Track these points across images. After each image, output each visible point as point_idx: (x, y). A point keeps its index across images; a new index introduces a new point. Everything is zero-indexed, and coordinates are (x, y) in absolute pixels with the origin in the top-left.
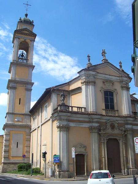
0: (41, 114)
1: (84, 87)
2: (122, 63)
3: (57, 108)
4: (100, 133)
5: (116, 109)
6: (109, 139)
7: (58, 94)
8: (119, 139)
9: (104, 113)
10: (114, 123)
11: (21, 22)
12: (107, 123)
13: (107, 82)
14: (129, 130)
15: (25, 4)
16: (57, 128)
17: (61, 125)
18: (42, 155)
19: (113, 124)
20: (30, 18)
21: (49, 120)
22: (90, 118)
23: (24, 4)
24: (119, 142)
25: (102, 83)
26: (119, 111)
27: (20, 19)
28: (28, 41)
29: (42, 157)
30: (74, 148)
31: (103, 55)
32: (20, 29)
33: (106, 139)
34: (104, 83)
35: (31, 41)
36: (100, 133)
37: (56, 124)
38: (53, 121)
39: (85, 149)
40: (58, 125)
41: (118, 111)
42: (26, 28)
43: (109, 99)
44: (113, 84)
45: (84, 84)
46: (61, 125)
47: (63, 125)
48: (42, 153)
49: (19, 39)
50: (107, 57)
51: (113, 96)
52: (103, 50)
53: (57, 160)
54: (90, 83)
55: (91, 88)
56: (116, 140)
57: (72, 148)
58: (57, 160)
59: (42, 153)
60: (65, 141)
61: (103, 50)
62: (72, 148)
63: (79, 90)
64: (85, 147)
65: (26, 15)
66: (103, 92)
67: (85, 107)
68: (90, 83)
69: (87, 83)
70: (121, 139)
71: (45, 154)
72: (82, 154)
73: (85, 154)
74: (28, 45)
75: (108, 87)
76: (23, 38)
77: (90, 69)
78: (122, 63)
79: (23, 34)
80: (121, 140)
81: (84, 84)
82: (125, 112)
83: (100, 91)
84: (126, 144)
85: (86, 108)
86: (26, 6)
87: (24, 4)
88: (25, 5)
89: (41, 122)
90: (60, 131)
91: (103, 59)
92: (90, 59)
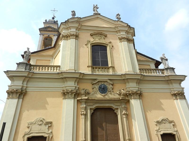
2: (120, 15)
4: (78, 98)
5: (110, 65)
9: (88, 71)
10: (105, 84)
11: (46, 22)
14: (133, 94)
15: (53, 10)
16: (6, 95)
20: (55, 20)
23: (51, 10)
24: (116, 113)
26: (115, 68)
27: (46, 21)
28: (51, 36)
31: (94, 10)
32: (45, 27)
33: (91, 109)
35: (54, 36)
39: (49, 127)
41: (113, 67)
42: (49, 26)
44: (106, 36)
49: (43, 35)
50: (99, 11)
51: (106, 50)
52: (94, 5)
55: (72, 42)
56: (111, 111)
61: (94, 5)
64: (50, 124)
65: (53, 18)
66: (89, 46)
68: (70, 37)
72: (42, 137)
73: (46, 135)
74: (52, 39)
75: (97, 40)
76: (47, 34)
77: (70, 21)
79: (47, 31)
80: (119, 110)
81: (63, 39)
82: (125, 69)
84: (127, 115)
85: (61, 67)
86: (53, 11)
87: (51, 10)
88: (52, 11)
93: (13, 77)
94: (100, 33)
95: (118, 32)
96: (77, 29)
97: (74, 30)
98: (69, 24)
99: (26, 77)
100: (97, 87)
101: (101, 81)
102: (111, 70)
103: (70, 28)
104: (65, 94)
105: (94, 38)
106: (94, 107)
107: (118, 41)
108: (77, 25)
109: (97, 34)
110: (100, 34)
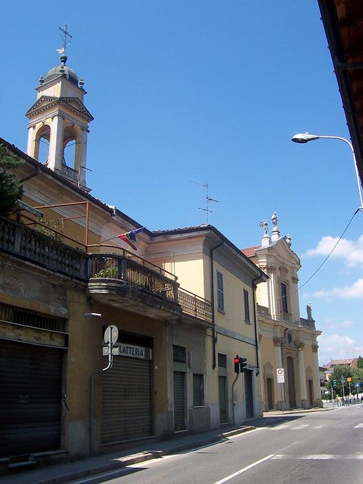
57: (278, 370)
62: (278, 370)
100: (287, 335)
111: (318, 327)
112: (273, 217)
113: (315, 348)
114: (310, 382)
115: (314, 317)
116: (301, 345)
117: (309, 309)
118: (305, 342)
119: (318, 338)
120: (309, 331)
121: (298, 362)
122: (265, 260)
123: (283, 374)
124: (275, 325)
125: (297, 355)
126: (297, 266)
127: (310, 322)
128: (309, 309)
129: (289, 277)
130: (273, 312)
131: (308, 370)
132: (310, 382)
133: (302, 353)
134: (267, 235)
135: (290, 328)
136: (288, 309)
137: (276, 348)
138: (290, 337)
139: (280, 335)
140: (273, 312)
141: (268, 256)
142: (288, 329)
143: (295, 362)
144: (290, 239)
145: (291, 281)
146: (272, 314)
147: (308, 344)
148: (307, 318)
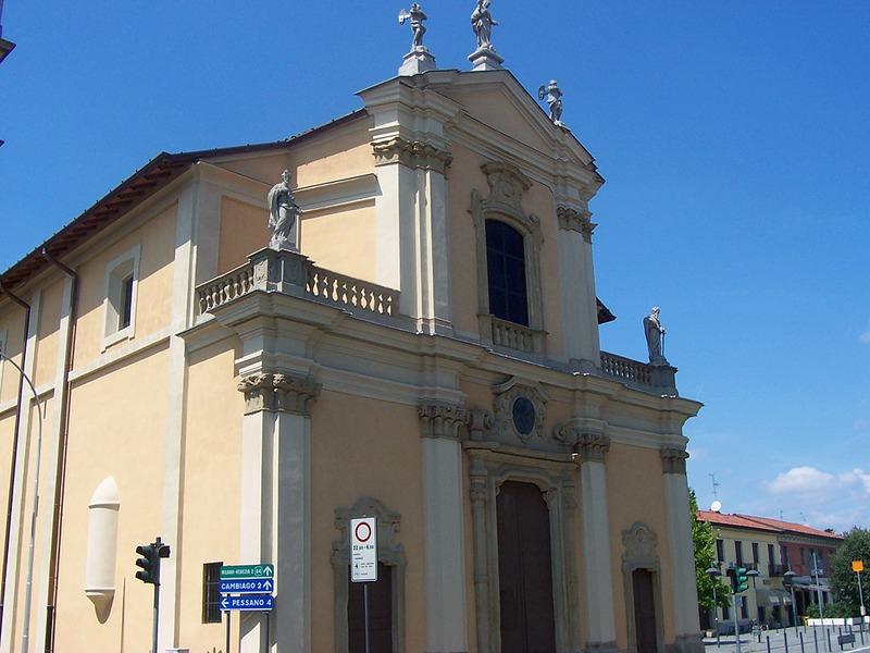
0: (65, 322)
1: (390, 177)
2: (560, 94)
3: (248, 272)
4: (470, 444)
6: (506, 482)
7: (231, 195)
8: (552, 485)
12: (498, 395)
13: (501, 171)
17: (278, 376)
18: (139, 563)
19: (526, 401)
21: (164, 344)
22: (422, 355)
25: (480, 172)
29: (139, 575)
30: (371, 521)
31: (478, 31)
34: (487, 173)
36: (470, 444)
37: (222, 373)
38: (192, 357)
40: (261, 375)
43: (504, 268)
44: (526, 188)
45: (396, 157)
46: (278, 376)
47: (288, 378)
48: (140, 550)
53: (233, 595)
54: (424, 157)
57: (355, 522)
58: (237, 594)
59: (140, 550)
60: (297, 475)
63: (360, 190)
67: (396, 286)
69: (410, 154)
70: (559, 489)
71: (150, 561)
78: (560, 94)
81: (396, 157)
83: (469, 212)
89: (69, 366)
90: (271, 409)
91: (479, 50)
92: (423, 30)
93: (279, 320)
94: (504, 171)
95: (560, 180)
96: (450, 126)
97: (438, 130)
98: (428, 96)
99: (321, 327)
100: (507, 404)
101: (519, 386)
102: (537, 341)
103: (424, 112)
104: (431, 417)
105: (491, 186)
106: (502, 479)
107: (555, 222)
108: (450, 109)
109: (501, 171)
110: (513, 175)
111: (685, 387)
112: (476, 12)
113: (674, 460)
114: (643, 584)
115: (671, 355)
116: (591, 446)
117: (652, 331)
118: (617, 437)
119: (690, 428)
120: (653, 403)
121: (572, 506)
122: (396, 123)
123: (372, 541)
124: (425, 353)
125: (571, 477)
126: (587, 178)
127: (657, 374)
128: (652, 331)
129: (538, 206)
130: (425, 309)
131: (636, 533)
132: (643, 584)
133: (594, 472)
134: (419, 49)
135: (527, 373)
136: (532, 311)
137: (428, 441)
138: (524, 414)
139: (447, 389)
140: (425, 309)
141: (409, 111)
142: (512, 376)
143: (555, 504)
144: (556, 92)
145: (550, 223)
146: (420, 315)
147: (633, 440)
148: (646, 361)
